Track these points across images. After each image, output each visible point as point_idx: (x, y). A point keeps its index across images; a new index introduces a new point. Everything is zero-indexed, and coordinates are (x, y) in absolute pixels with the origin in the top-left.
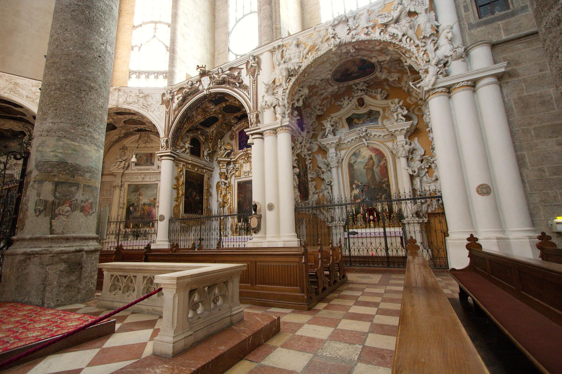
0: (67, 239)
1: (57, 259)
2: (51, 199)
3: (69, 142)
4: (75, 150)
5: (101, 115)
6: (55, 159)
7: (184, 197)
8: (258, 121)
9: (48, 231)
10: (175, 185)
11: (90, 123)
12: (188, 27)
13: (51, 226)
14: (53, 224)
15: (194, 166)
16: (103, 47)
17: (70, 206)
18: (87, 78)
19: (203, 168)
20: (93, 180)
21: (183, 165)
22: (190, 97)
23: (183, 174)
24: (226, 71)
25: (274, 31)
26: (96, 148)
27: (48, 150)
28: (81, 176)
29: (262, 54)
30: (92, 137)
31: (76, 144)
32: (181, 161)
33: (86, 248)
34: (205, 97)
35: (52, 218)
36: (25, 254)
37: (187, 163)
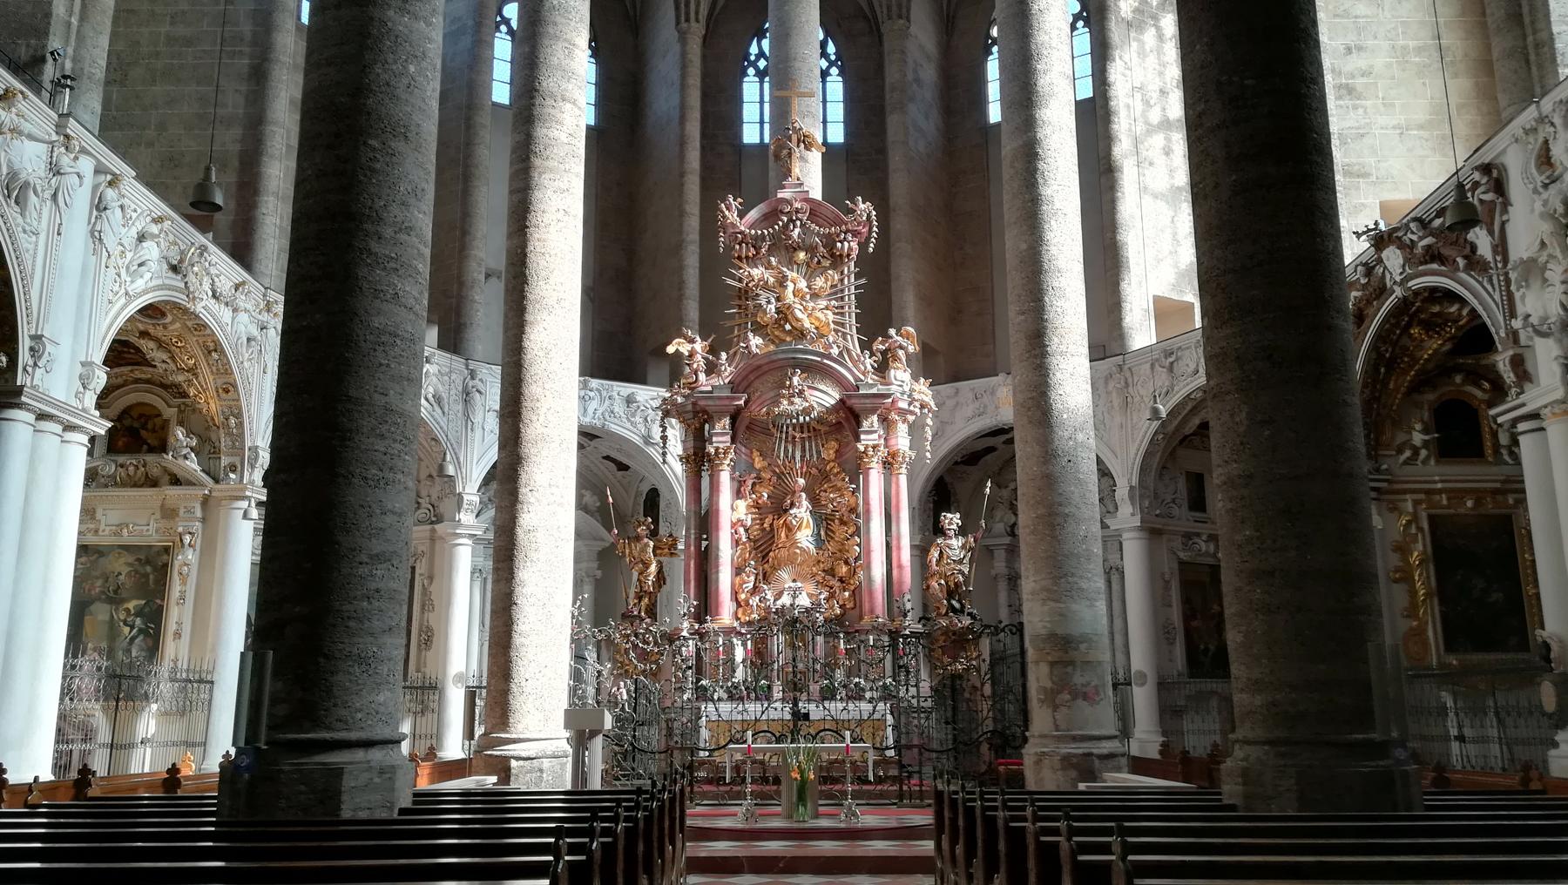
2: (1049, 685)
3: (1052, 604)
4: (1061, 615)
5: (1087, 550)
6: (1043, 632)
7: (1436, 601)
8: (1524, 375)
10: (1396, 571)
12: (1360, 49)
15: (1457, 495)
17: (1070, 693)
19: (1504, 492)
21: (1416, 503)
22: (1370, 311)
23: (1420, 529)
24: (1432, 220)
25: (1532, 57)
26: (1088, 603)
29: (1504, 152)
30: (1083, 590)
31: (1062, 606)
32: (1405, 492)
33: (1095, 751)
34: (1403, 306)
36: (1036, 754)
37: (1428, 492)
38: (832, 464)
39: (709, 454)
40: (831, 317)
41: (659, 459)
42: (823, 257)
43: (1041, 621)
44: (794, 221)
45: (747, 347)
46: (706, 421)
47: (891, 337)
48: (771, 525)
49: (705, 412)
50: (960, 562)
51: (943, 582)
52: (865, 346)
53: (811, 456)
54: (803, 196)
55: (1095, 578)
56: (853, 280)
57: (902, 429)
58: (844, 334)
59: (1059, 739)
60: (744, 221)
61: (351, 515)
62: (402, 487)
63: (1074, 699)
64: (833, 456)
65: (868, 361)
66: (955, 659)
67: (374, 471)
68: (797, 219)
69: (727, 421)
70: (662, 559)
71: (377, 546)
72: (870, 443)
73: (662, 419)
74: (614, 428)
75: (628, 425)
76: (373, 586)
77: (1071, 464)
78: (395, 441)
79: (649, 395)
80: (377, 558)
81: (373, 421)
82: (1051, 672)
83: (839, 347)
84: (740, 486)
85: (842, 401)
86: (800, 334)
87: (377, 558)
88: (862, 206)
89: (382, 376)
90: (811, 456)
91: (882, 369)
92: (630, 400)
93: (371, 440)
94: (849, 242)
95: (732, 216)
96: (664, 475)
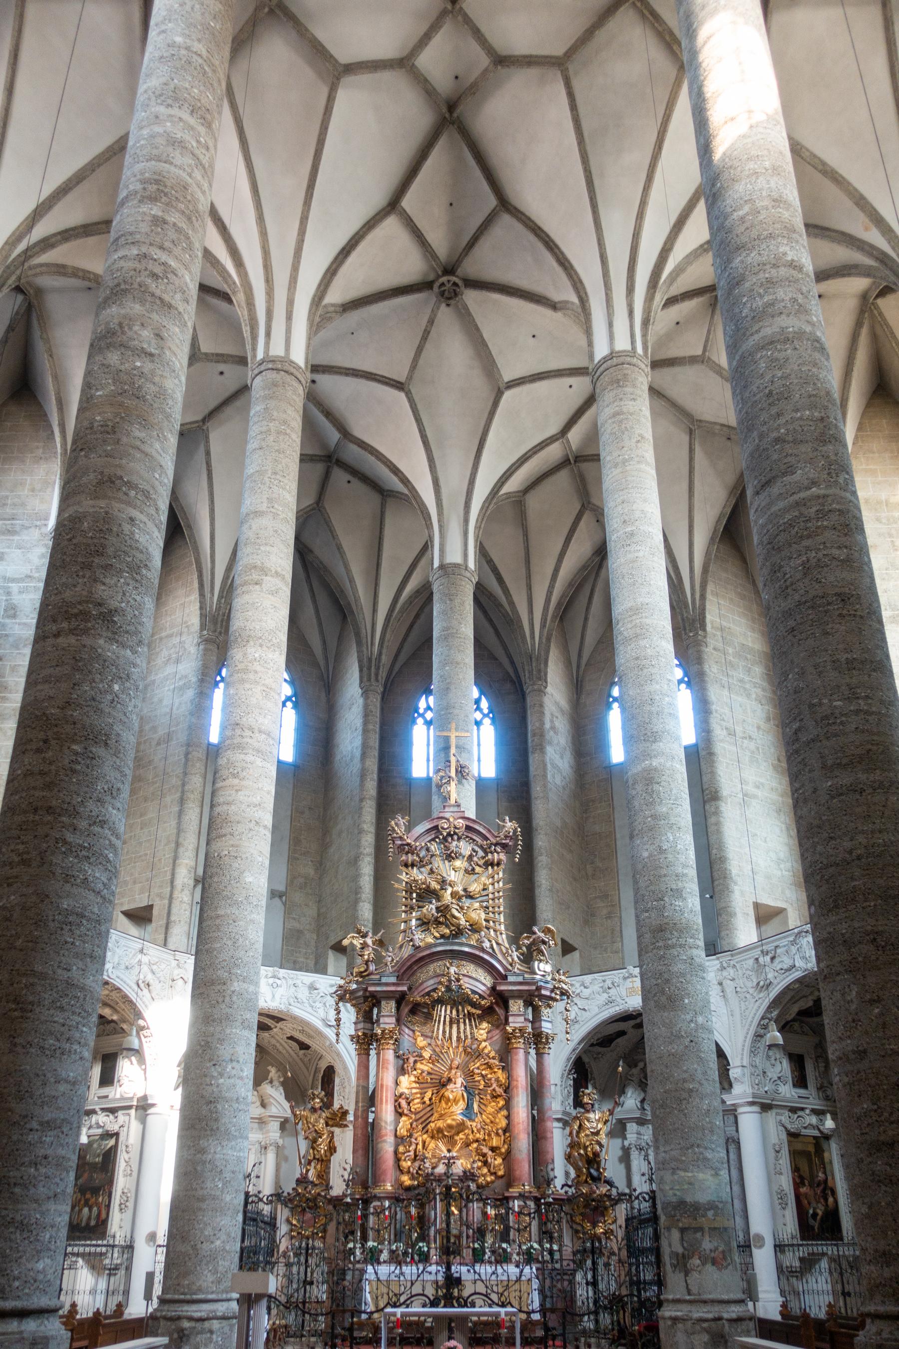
0: (705, 1302)
1: (698, 1327)
2: (680, 1250)
3: (682, 1174)
4: (690, 1184)
5: (710, 1122)
6: (674, 1199)
9: (685, 1292)
11: (698, 1142)
13: (687, 1285)
14: (689, 1282)
16: (693, 1025)
17: (700, 1258)
18: (685, 1081)
20: (718, 1218)
26: (713, 1172)
27: (668, 1188)
28: (703, 1216)
30: (706, 1159)
31: (690, 1174)
35: (686, 1275)
36: (671, 1318)
38: (484, 1044)
39: (376, 1035)
40: (483, 916)
41: (333, 1038)
42: (478, 865)
43: (672, 1189)
44: (452, 836)
45: (412, 940)
46: (374, 1005)
47: (535, 933)
48: (430, 1099)
49: (373, 995)
50: (597, 1133)
51: (582, 1152)
52: (514, 941)
53: (466, 1037)
54: (459, 815)
55: (719, 1149)
56: (501, 884)
57: (545, 1012)
58: (495, 931)
59: (690, 1302)
60: (409, 835)
61: (25, 1083)
62: (78, 1057)
63: (704, 1264)
64: (485, 1036)
65: (515, 954)
66: (594, 1225)
67: (51, 1041)
68: (455, 833)
69: (393, 1004)
70: (333, 1129)
71: (48, 1114)
72: (517, 1025)
73: (337, 1004)
74: (297, 1012)
75: (310, 1010)
76: (42, 1152)
77: (693, 1044)
78: (74, 1013)
79: (328, 983)
80: (48, 1125)
81: (55, 995)
82: (682, 1239)
83: (490, 941)
84: (404, 1063)
85: (493, 989)
86: (458, 932)
87: (48, 1125)
88: (509, 824)
89: (66, 953)
90: (466, 1037)
91: (528, 959)
92: (312, 988)
93: (52, 1012)
94: (498, 853)
95: (400, 830)
96: (339, 1054)
